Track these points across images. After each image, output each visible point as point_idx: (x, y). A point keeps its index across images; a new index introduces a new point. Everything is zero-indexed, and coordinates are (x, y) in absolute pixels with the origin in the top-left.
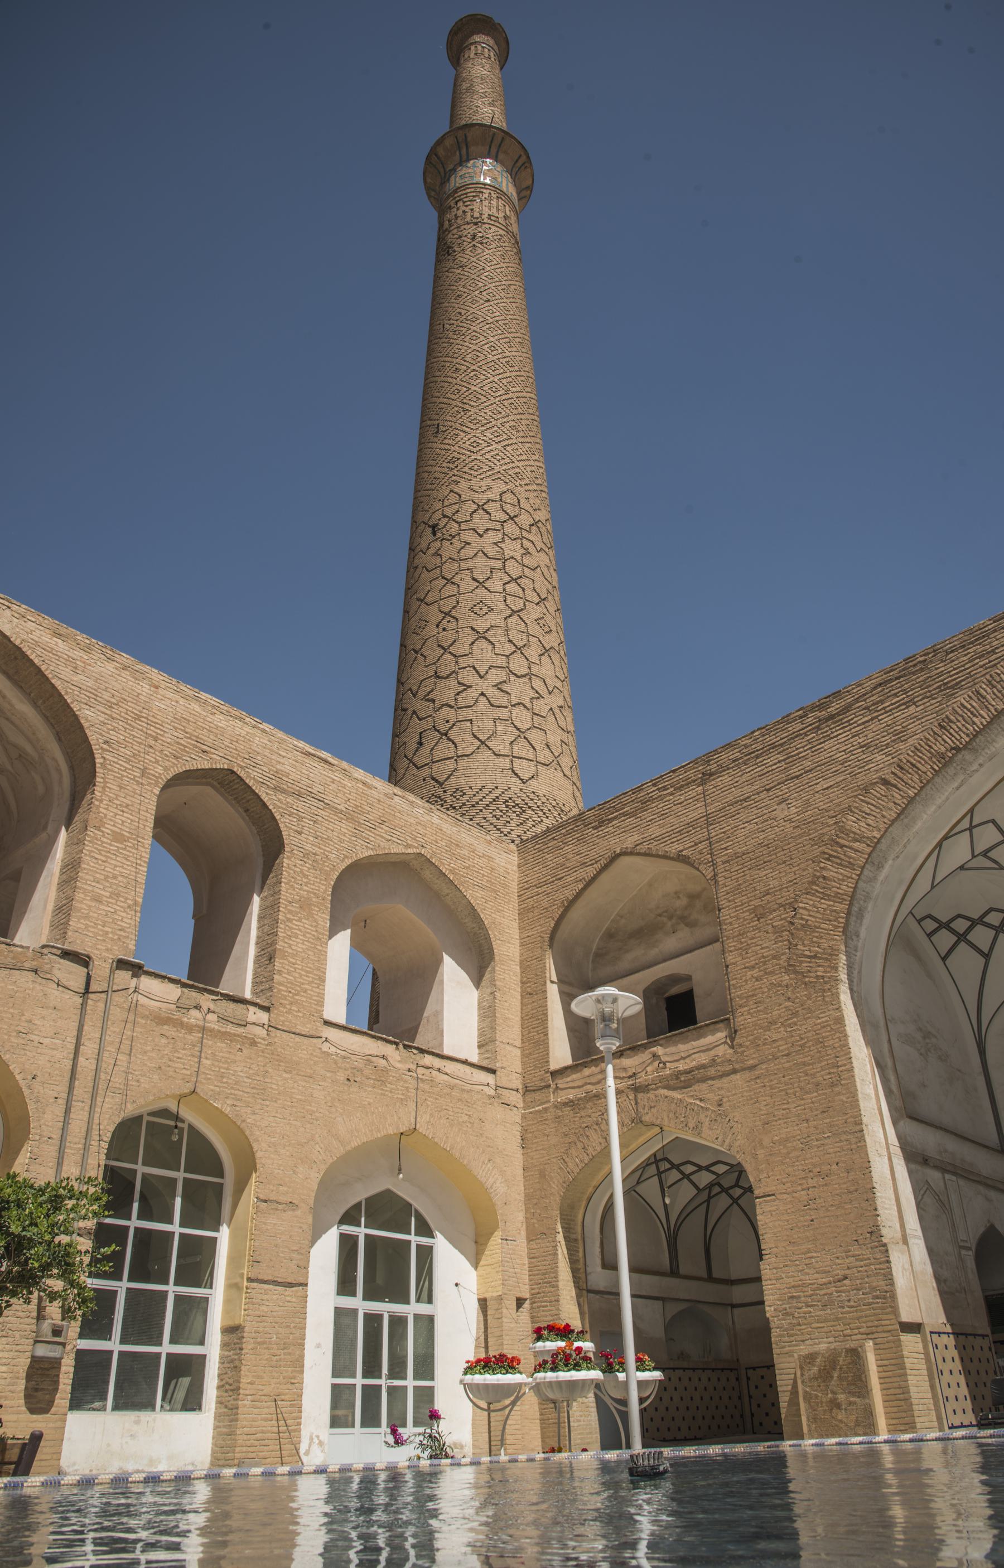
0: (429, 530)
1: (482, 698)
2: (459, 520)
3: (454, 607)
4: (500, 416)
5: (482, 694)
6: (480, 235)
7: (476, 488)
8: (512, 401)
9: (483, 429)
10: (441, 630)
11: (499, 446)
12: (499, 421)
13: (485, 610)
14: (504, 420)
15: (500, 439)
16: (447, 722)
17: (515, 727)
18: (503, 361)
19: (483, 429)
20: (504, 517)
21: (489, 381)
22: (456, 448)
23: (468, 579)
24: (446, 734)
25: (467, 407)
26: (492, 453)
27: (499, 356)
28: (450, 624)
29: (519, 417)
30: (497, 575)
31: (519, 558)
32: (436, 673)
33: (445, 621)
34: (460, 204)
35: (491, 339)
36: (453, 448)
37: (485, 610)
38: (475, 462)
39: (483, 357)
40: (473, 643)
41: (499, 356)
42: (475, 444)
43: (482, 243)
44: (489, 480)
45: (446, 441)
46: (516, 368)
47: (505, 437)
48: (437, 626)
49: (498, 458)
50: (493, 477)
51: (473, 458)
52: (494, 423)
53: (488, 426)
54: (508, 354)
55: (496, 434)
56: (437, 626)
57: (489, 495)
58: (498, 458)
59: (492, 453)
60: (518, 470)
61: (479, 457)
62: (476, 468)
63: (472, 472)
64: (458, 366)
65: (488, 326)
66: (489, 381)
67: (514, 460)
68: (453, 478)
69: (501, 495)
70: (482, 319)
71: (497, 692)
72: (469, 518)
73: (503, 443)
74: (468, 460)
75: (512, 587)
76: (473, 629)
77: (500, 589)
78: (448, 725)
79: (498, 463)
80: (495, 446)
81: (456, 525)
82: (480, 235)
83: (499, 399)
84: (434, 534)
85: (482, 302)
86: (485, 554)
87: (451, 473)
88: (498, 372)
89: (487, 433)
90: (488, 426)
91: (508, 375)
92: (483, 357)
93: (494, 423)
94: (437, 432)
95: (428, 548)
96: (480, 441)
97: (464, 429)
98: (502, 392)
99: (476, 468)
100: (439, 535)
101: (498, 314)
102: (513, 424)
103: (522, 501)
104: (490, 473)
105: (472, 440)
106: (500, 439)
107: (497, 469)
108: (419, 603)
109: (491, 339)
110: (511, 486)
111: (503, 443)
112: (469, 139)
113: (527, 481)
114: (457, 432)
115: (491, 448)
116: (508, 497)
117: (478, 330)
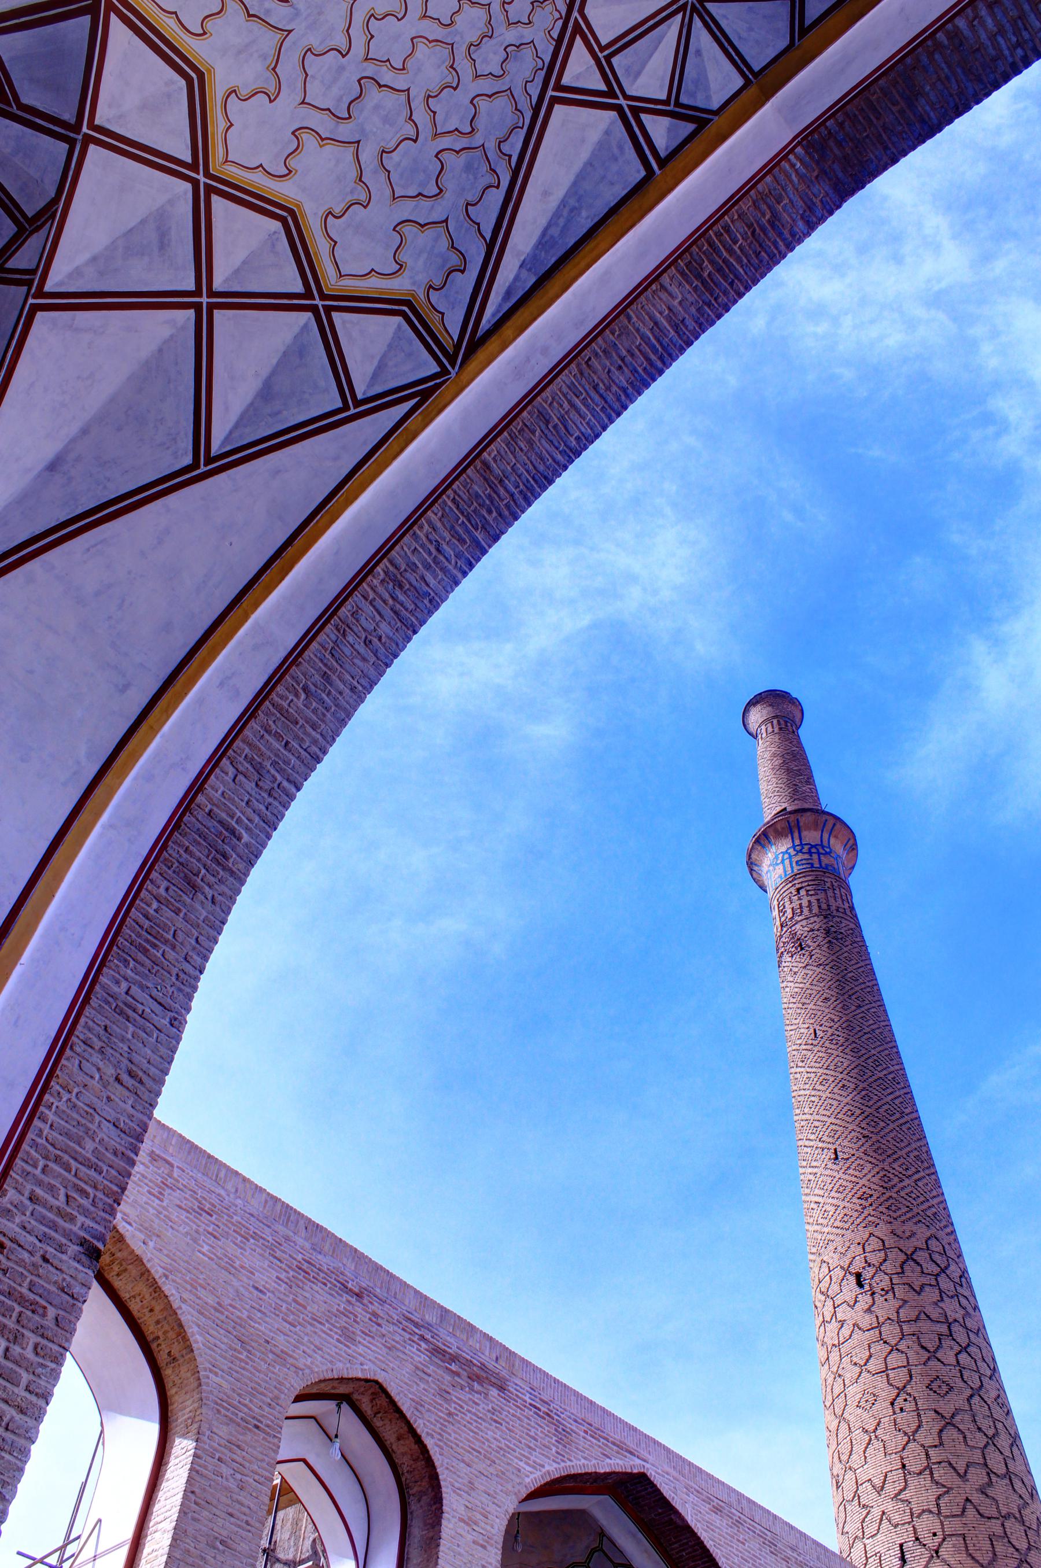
0: (852, 1280)
1: (969, 1506)
2: (889, 1271)
3: (909, 1382)
5: (967, 1500)
6: (833, 929)
7: (899, 1233)
9: (890, 1160)
10: (898, 1410)
13: (945, 1388)
16: (935, 1534)
17: (1014, 1547)
19: (890, 1160)
20: (936, 1270)
23: (916, 1347)
24: (937, 1552)
26: (907, 1190)
27: (885, 1072)
28: (907, 1404)
30: (947, 1343)
31: (961, 1320)
32: (904, 1466)
33: (900, 1400)
34: (803, 892)
35: (873, 1052)
36: (862, 1182)
37: (945, 1388)
38: (891, 1201)
39: (870, 1074)
40: (941, 1431)
41: (885, 1072)
42: (886, 1179)
43: (837, 939)
44: (910, 1223)
45: (849, 1172)
48: (892, 1404)
49: (914, 1196)
50: (914, 1220)
52: (900, 1153)
53: (895, 1156)
54: (892, 1069)
55: (904, 1167)
56: (892, 1404)
57: (915, 1242)
59: (907, 1190)
61: (895, 1195)
62: (893, 1208)
63: (891, 1213)
64: (845, 1083)
68: (870, 1218)
69: (926, 1242)
70: (858, 1029)
71: (982, 1497)
72: (899, 1270)
75: (963, 1357)
76: (936, 1412)
77: (953, 1361)
78: (938, 1539)
79: (913, 1201)
81: (887, 1277)
82: (833, 929)
84: (860, 1284)
85: (853, 1008)
86: (928, 1316)
88: (889, 1091)
89: (895, 1165)
90: (895, 1156)
92: (870, 1074)
94: (836, 1158)
95: (856, 1302)
96: (892, 1176)
97: (870, 1159)
98: (898, 1115)
100: (867, 1288)
101: (871, 1022)
103: (947, 1247)
104: (909, 1215)
105: (882, 1174)
108: (857, 1369)
110: (933, 1231)
112: (801, 824)
114: (862, 1162)
116: (933, 1243)
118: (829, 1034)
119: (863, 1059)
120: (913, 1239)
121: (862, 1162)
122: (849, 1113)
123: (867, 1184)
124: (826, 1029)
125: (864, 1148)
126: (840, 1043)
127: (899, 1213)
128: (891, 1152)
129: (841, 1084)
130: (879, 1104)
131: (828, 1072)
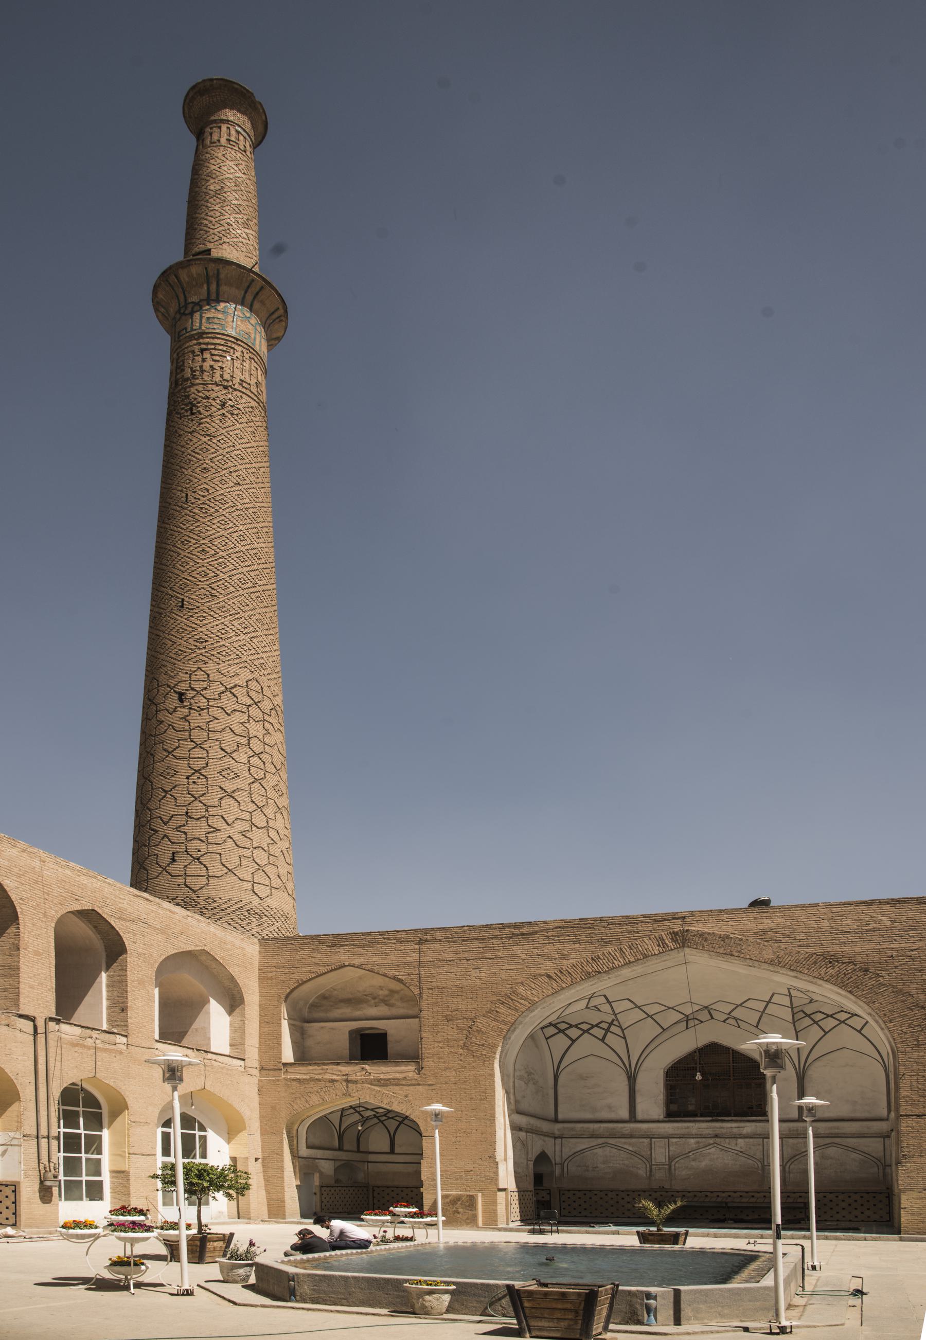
4: (247, 608)
7: (224, 672)
8: (258, 594)
9: (231, 618)
11: (247, 637)
12: (247, 614)
14: (251, 613)
15: (247, 631)
18: (252, 552)
21: (237, 571)
22: (203, 629)
25: (215, 592)
26: (240, 643)
27: (248, 547)
29: (264, 610)
35: (241, 528)
41: (248, 547)
44: (236, 667)
46: (263, 561)
47: (252, 629)
49: (245, 648)
51: (221, 643)
52: (242, 614)
54: (256, 545)
55: (244, 625)
57: (236, 681)
58: (245, 648)
60: (262, 661)
61: (227, 645)
63: (220, 657)
64: (206, 548)
65: (238, 513)
66: (237, 571)
67: (259, 651)
68: (201, 657)
70: (232, 504)
73: (251, 635)
74: (216, 645)
80: (243, 637)
83: (247, 591)
85: (231, 484)
87: (199, 652)
89: (235, 623)
90: (236, 616)
91: (255, 567)
92: (233, 546)
93: (242, 614)
96: (229, 630)
98: (250, 585)
99: (224, 653)
101: (247, 501)
102: (259, 617)
103: (265, 689)
104: (238, 661)
105: (220, 627)
106: (247, 631)
107: (244, 659)
109: (241, 528)
110: (256, 675)
111: (251, 635)
113: (269, 671)
114: (205, 615)
115: (239, 638)
116: (253, 684)
117: (227, 515)
118: (199, 502)
119: (228, 531)
120: (235, 678)
121: (205, 615)
122: (203, 574)
123: (205, 631)
124: (198, 496)
125: (209, 604)
126: (209, 513)
127: (227, 658)
128: (234, 612)
129: (201, 549)
130: (235, 572)
131: (191, 535)
